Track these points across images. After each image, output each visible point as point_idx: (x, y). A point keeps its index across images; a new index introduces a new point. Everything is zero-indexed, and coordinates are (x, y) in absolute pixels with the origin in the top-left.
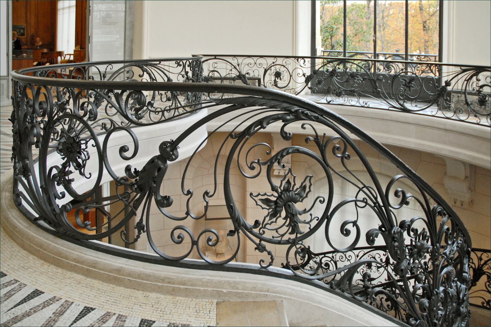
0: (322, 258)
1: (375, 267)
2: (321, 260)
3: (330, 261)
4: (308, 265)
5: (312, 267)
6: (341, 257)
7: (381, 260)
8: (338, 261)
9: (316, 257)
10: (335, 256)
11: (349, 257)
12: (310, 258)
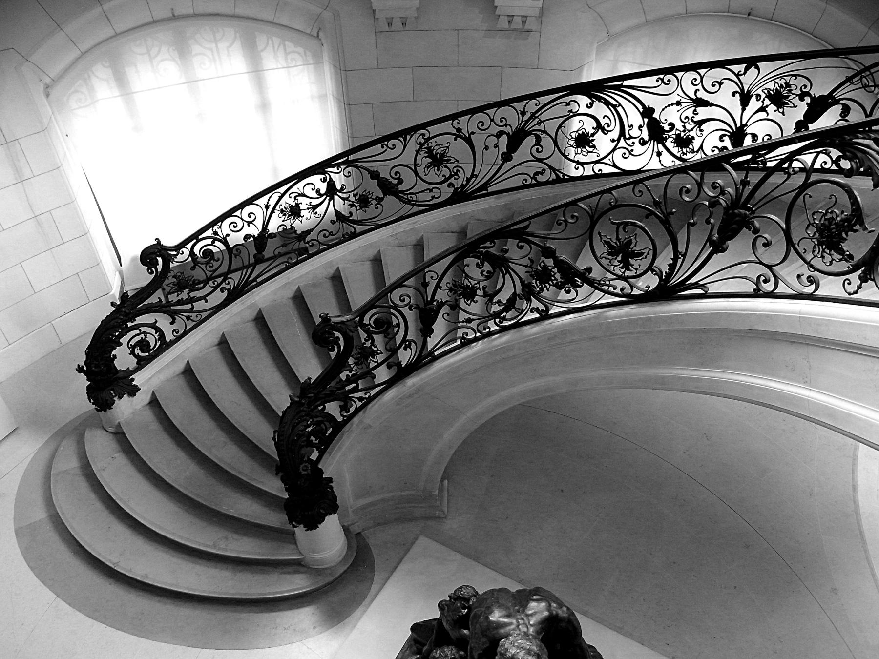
1: (308, 209)
3: (212, 245)
7: (318, 192)
12: (167, 260)
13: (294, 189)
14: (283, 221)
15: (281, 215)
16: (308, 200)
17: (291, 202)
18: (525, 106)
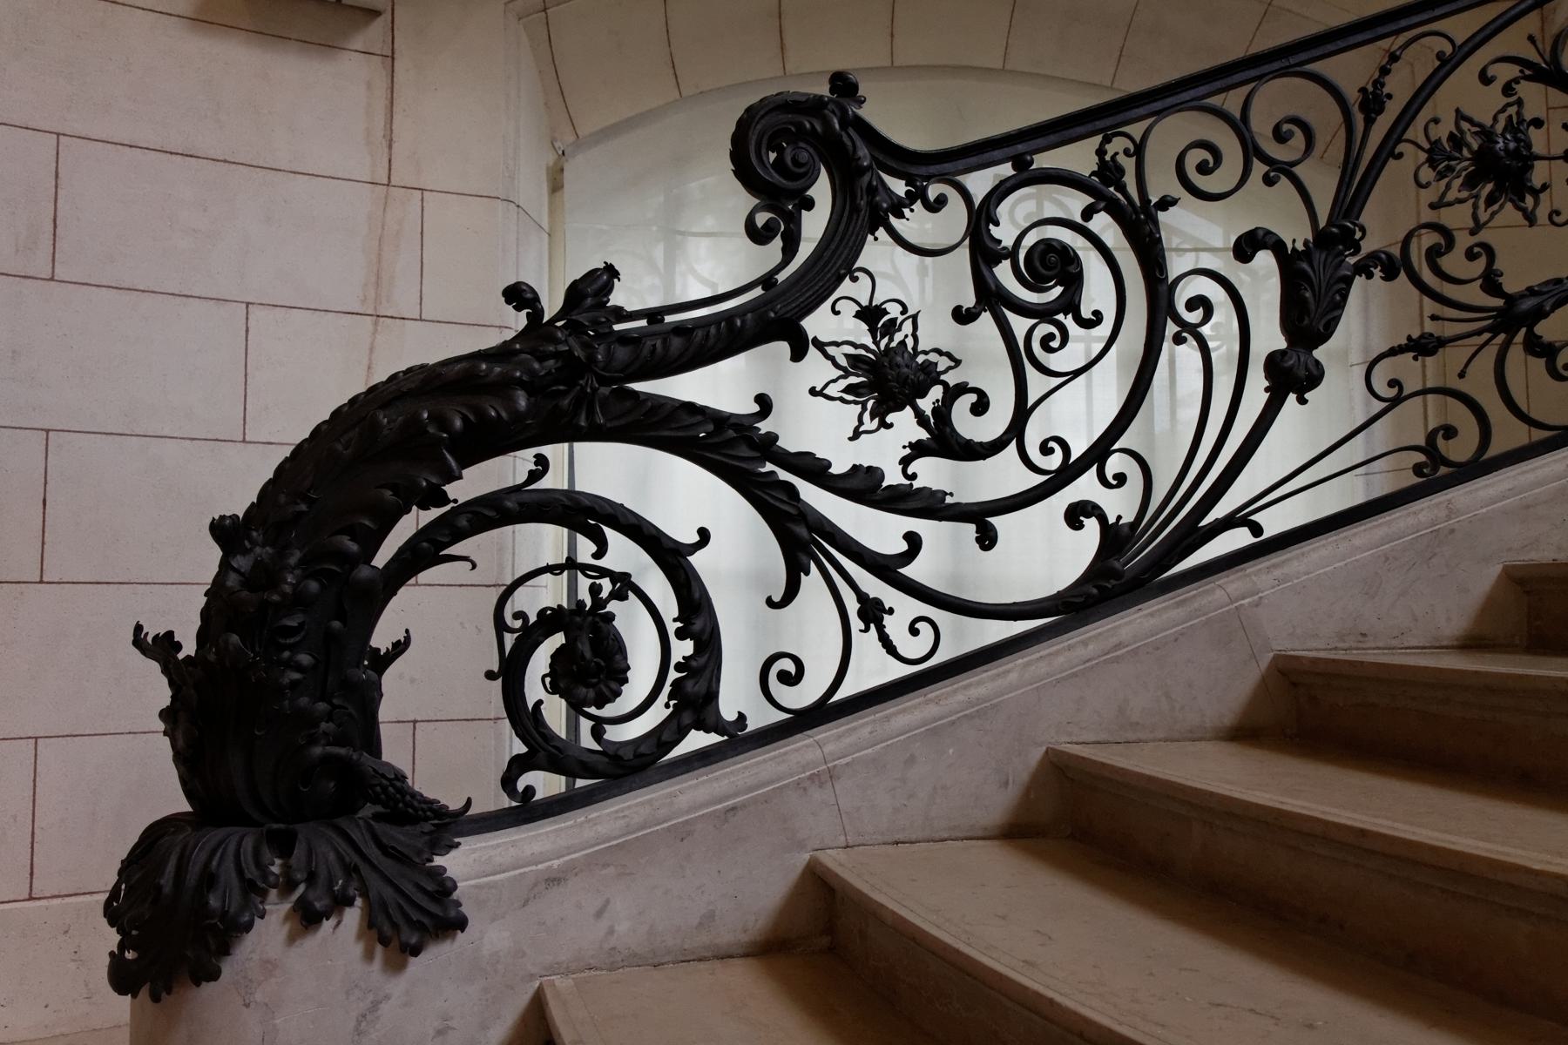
0: (1001, 191)
2: (981, 216)
4: (846, 287)
5: (894, 311)
6: (1196, 157)
8: (1166, 203)
9: (933, 191)
10: (1129, 164)
14: (1433, 206)
15: (1427, 174)
17: (1485, 105)
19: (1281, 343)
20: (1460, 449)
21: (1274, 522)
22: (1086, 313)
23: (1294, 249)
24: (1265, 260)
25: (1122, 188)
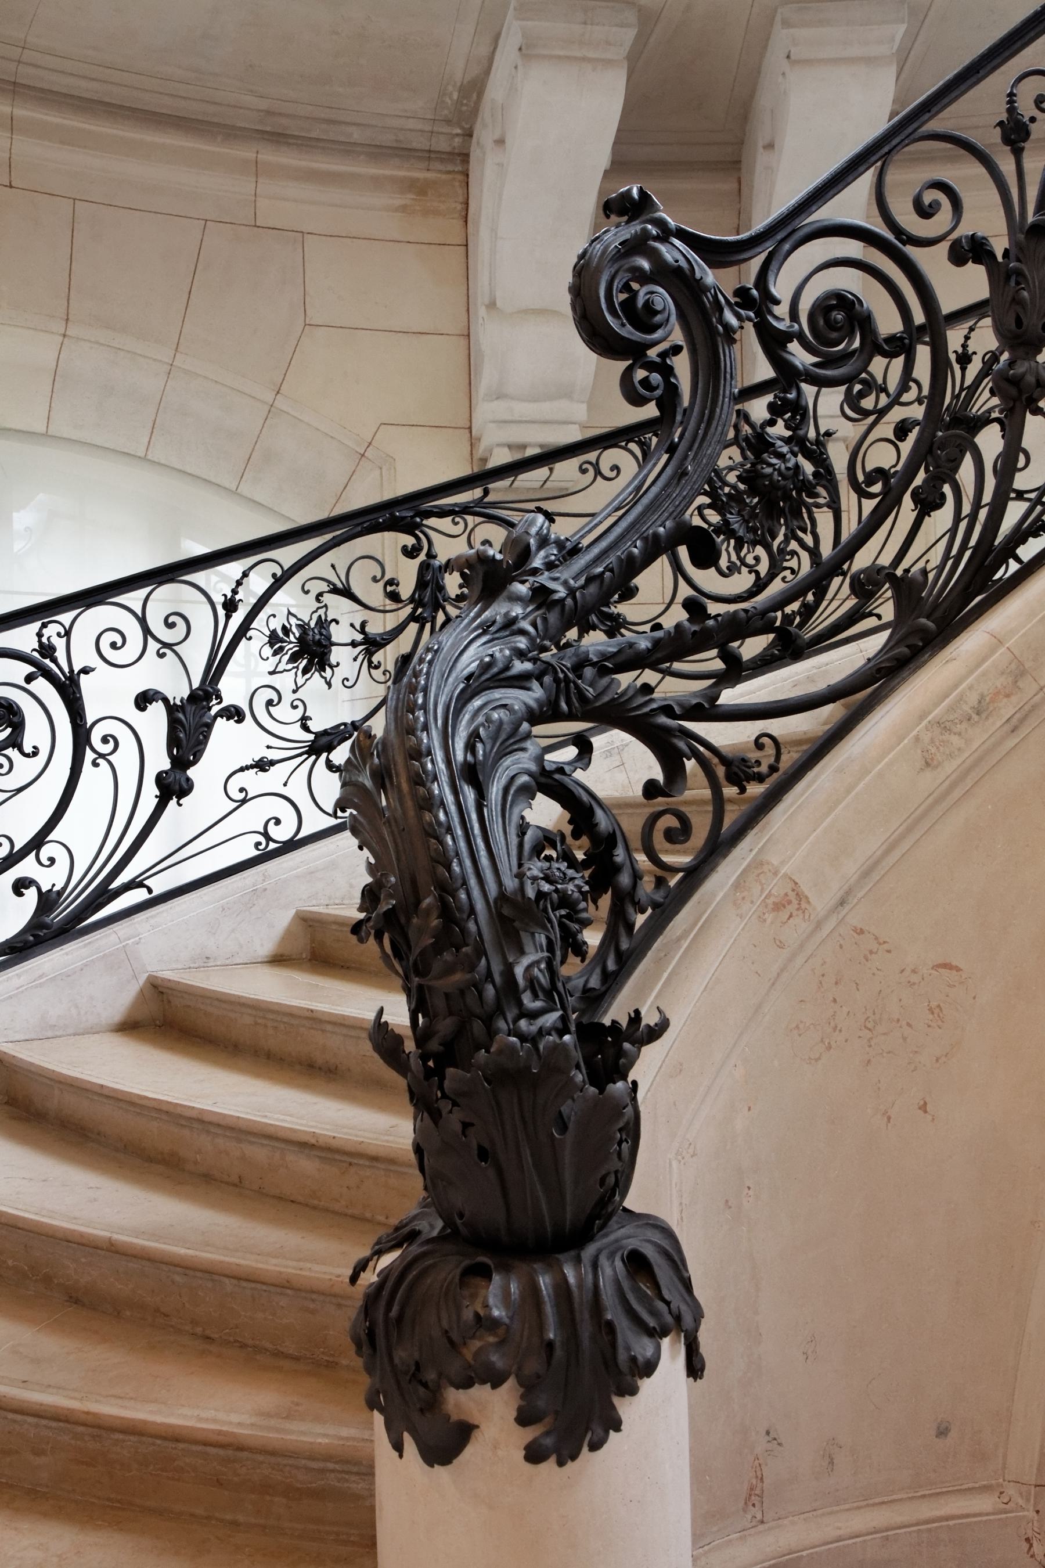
1: (354, 644)
8: (86, 671)
10: (60, 644)
11: (171, 626)
13: (320, 567)
14: (271, 673)
15: (268, 651)
16: (359, 615)
18: (967, 338)
19: (166, 764)
20: (282, 833)
21: (159, 885)
22: (28, 749)
23: (174, 704)
24: (157, 710)
25: (54, 661)
